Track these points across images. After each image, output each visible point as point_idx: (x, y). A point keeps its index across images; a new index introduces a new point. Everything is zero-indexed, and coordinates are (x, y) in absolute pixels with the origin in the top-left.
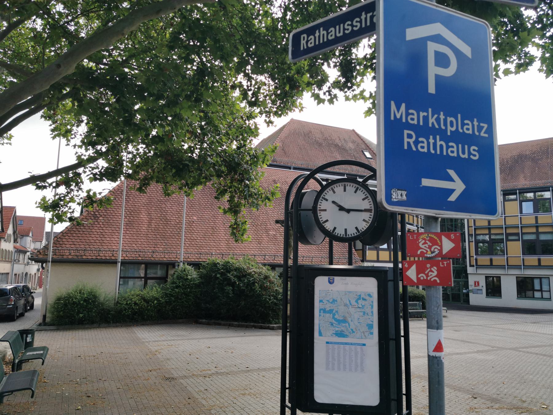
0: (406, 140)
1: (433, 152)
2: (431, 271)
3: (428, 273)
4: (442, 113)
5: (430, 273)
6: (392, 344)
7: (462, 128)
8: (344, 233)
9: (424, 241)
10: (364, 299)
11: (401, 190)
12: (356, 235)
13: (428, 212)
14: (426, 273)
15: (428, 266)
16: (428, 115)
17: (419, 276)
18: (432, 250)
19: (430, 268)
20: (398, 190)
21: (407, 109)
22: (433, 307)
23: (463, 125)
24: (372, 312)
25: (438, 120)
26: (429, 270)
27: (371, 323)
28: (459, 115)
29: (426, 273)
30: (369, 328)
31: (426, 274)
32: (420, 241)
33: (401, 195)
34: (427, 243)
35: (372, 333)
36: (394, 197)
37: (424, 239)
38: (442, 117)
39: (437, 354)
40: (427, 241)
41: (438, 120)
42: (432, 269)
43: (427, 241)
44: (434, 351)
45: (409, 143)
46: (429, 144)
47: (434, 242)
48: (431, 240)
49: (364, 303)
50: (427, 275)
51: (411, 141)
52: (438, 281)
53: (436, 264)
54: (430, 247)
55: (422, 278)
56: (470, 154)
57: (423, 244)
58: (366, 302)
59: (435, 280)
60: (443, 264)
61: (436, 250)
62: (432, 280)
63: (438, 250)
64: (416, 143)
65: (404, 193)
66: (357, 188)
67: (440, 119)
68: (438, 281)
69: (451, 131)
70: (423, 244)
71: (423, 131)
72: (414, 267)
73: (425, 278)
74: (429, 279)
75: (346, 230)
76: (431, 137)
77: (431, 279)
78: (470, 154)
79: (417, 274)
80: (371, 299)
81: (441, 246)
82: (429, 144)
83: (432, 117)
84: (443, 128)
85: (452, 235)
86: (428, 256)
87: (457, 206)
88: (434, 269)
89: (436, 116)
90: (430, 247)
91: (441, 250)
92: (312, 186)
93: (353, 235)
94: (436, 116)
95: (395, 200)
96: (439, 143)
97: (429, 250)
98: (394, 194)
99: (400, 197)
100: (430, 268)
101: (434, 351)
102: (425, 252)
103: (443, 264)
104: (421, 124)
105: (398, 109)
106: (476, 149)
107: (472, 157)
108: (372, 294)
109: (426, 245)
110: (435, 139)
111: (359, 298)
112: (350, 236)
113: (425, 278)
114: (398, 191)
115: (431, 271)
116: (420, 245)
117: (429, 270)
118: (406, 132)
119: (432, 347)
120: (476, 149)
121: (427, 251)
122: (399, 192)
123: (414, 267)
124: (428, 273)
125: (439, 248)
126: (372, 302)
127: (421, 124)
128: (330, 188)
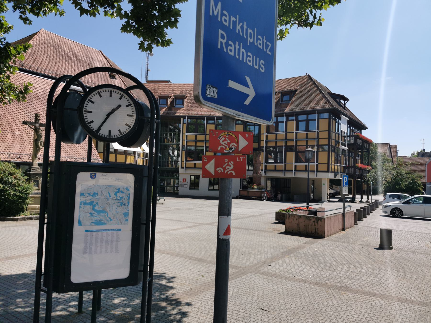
0: (220, 39)
1: (237, 57)
2: (229, 165)
3: (226, 167)
4: (245, 23)
5: (227, 167)
6: (144, 228)
7: (257, 42)
8: (108, 135)
9: (224, 138)
10: (122, 192)
11: (214, 87)
12: (118, 136)
13: (231, 112)
14: (224, 167)
15: (226, 160)
16: (236, 20)
17: (217, 170)
18: (230, 146)
19: (228, 162)
20: (212, 87)
21: (222, 9)
22: (226, 197)
23: (258, 39)
24: (129, 203)
25: (242, 27)
26: (227, 164)
27: (127, 212)
28: (256, 29)
29: (224, 167)
30: (125, 216)
31: (223, 168)
32: (221, 138)
33: (214, 92)
34: (227, 141)
35: (127, 220)
36: (208, 93)
37: (224, 136)
38: (245, 27)
39: (226, 237)
40: (227, 139)
41: (242, 27)
42: (230, 163)
43: (227, 139)
44: (224, 235)
45: (221, 43)
46: (235, 48)
47: (233, 140)
48: (230, 138)
49: (122, 195)
50: (224, 169)
51: (224, 41)
52: (234, 174)
53: (233, 159)
54: (229, 144)
55: (220, 172)
56: (260, 66)
57: (223, 141)
58: (124, 195)
59: (232, 173)
60: (239, 159)
61: (233, 147)
62: (229, 173)
63: (235, 147)
64: (227, 45)
65: (216, 90)
66: (122, 96)
67: (244, 27)
68: (234, 174)
69: (250, 42)
70: (223, 141)
71: (233, 36)
72: (213, 161)
73: (223, 171)
74: (226, 172)
75: (110, 131)
76: (237, 42)
77: (227, 172)
78: (260, 66)
79: (216, 168)
80: (128, 192)
81: (238, 144)
82: (235, 48)
83: (239, 25)
84: (245, 37)
85: (247, 135)
86: (227, 152)
87: (247, 110)
88: (231, 163)
89: (241, 24)
90: (229, 144)
91: (237, 147)
92: (102, 78)
93: (116, 137)
94: (241, 24)
95: (209, 96)
96: (242, 50)
97: (227, 146)
98: (208, 90)
99: (212, 94)
100: (228, 162)
101: (224, 235)
102: (224, 148)
103: (239, 159)
104: (231, 28)
105: (216, 7)
106: (264, 63)
107: (260, 69)
108: (129, 188)
109: (226, 142)
110: (239, 45)
111: (118, 191)
112: (113, 137)
113: (223, 171)
114: (212, 88)
115: (229, 165)
116: (221, 141)
117: (227, 164)
118: (220, 31)
119: (222, 232)
120: (264, 63)
121: (226, 147)
122: (212, 89)
123: (213, 161)
124: (226, 167)
125: (236, 145)
126: (129, 194)
127: (231, 28)
128: (96, 92)
